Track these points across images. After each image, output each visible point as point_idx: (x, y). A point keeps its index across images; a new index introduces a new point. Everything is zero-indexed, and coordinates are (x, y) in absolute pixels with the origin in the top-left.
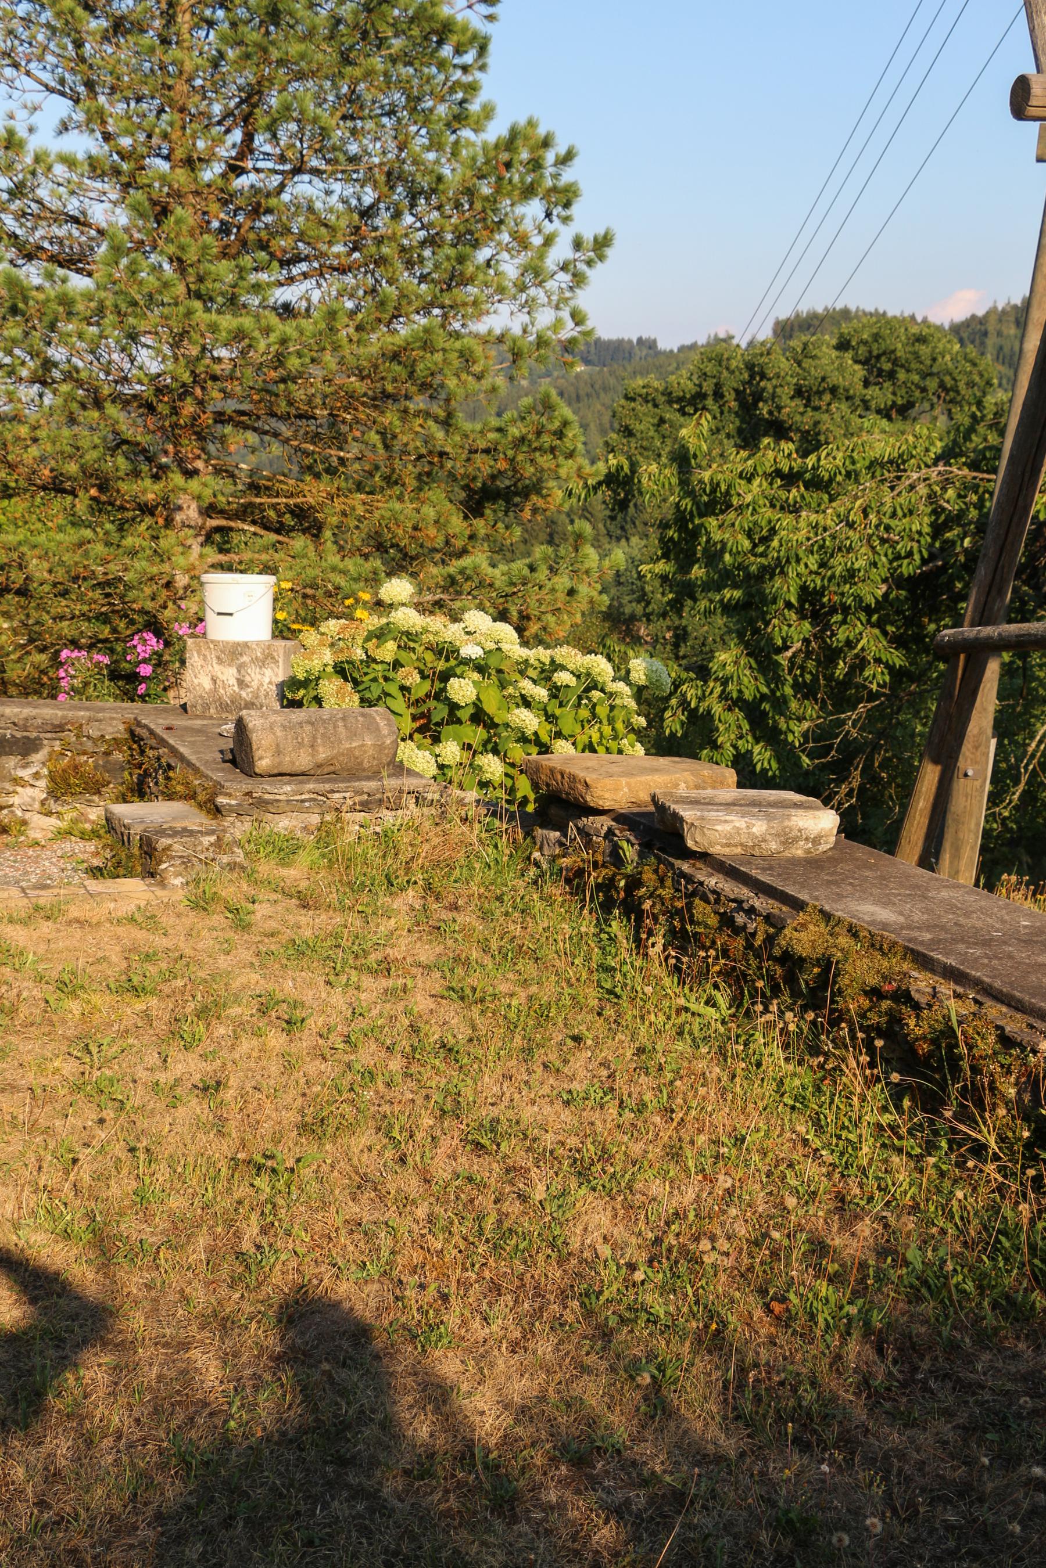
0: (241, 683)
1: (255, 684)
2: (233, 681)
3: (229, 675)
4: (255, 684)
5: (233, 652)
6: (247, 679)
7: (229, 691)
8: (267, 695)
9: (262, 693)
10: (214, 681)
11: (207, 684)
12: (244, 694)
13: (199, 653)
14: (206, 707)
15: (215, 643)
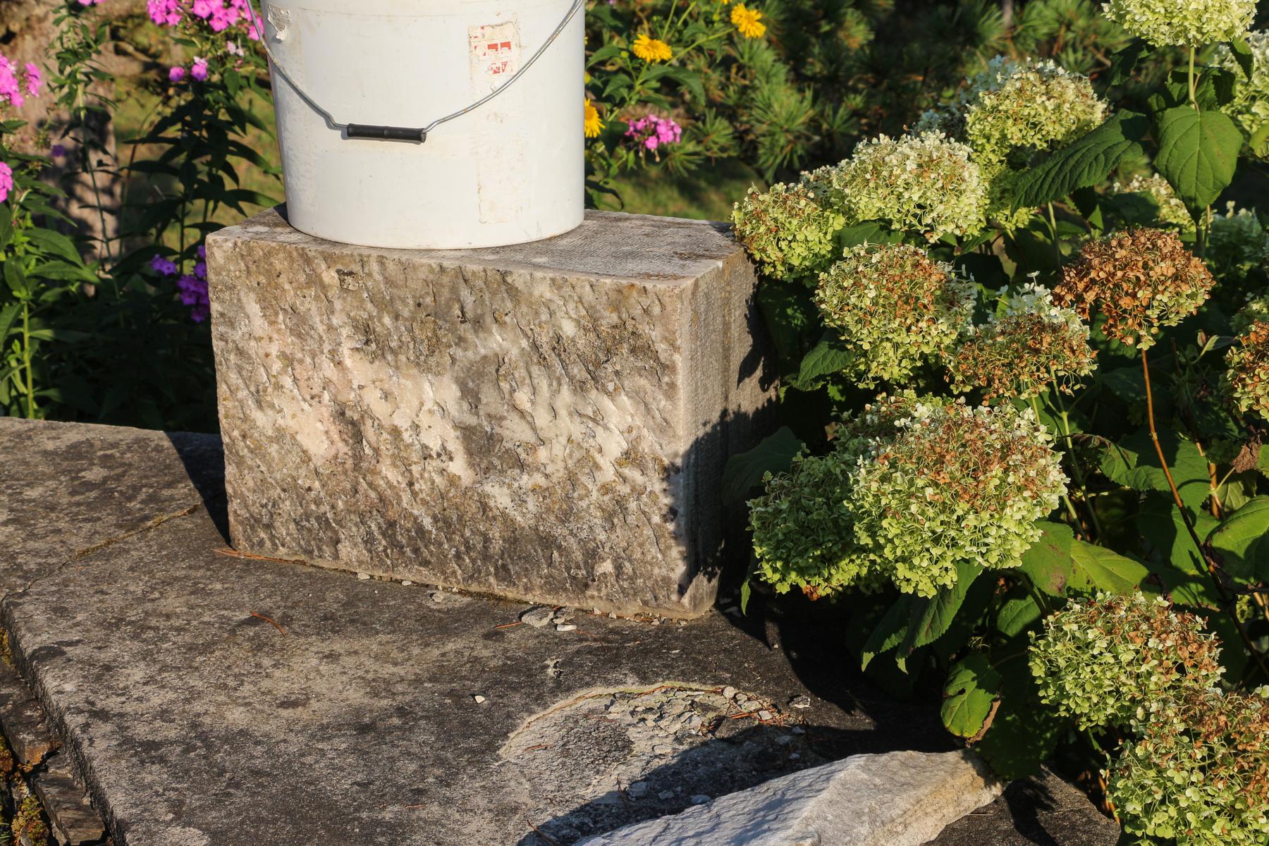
0: (483, 445)
1: (553, 458)
2: (439, 434)
3: (422, 408)
4: (553, 458)
5: (439, 308)
6: (515, 431)
7: (429, 477)
8: (615, 511)
9: (591, 499)
10: (351, 424)
11: (317, 437)
12: (500, 497)
13: (269, 306)
14: (325, 531)
15: (349, 263)
